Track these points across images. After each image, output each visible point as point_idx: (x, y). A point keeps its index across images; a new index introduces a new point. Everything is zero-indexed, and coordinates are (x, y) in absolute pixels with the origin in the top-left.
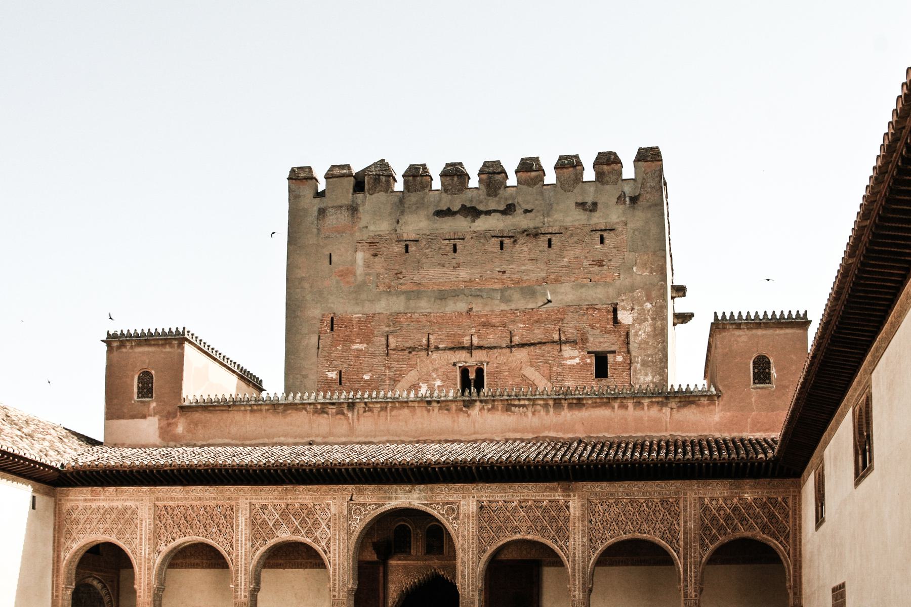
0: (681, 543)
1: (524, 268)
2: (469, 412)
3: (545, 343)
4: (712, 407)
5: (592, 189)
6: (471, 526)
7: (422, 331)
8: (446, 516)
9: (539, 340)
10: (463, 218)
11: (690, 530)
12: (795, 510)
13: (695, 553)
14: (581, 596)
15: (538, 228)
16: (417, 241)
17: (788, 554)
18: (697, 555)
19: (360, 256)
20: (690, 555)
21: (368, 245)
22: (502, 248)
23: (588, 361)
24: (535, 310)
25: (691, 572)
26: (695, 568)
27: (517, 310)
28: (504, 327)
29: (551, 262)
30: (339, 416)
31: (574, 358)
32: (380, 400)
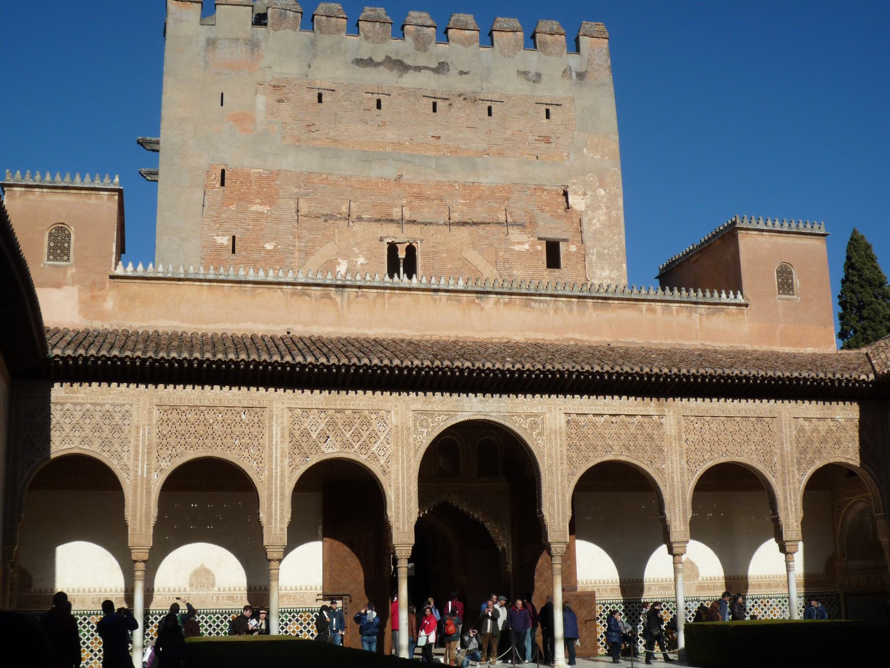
0: (778, 467)
1: (461, 135)
2: (482, 305)
3: (489, 223)
7: (341, 197)
8: (529, 431)
9: (483, 220)
11: (787, 453)
13: (793, 479)
14: (682, 529)
15: (477, 93)
16: (334, 90)
20: (789, 481)
22: (435, 110)
23: (539, 248)
24: (476, 184)
25: (790, 499)
29: (493, 132)
30: (324, 301)
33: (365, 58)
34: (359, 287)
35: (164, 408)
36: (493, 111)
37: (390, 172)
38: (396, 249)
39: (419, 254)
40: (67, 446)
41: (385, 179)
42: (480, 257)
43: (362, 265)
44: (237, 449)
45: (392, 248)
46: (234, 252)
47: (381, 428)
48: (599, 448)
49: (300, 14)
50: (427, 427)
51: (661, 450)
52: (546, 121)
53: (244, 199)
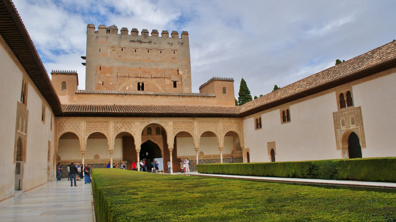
3: (160, 78)
4: (214, 99)
6: (171, 128)
10: (137, 43)
21: (111, 47)
22: (148, 52)
23: (172, 83)
26: (222, 138)
30: (122, 97)
31: (168, 82)
34: (130, 94)
35: (88, 122)
37: (138, 66)
38: (140, 84)
39: (144, 85)
40: (67, 130)
43: (132, 87)
44: (103, 130)
45: (139, 84)
46: (103, 85)
48: (180, 129)
50: (143, 125)
51: (193, 129)
52: (174, 54)
53: (105, 73)
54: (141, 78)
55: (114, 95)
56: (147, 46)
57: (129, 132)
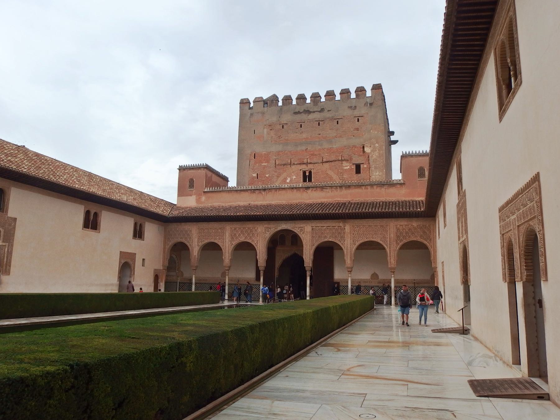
0: (388, 242)
1: (328, 132)
3: (336, 161)
5: (354, 101)
12: (433, 230)
17: (431, 247)
18: (395, 247)
19: (265, 130)
20: (392, 247)
21: (268, 126)
22: (319, 125)
23: (353, 167)
25: (392, 253)
26: (394, 252)
27: (325, 148)
28: (320, 155)
30: (260, 194)
31: (347, 166)
32: (274, 188)
33: (297, 111)
36: (339, 122)
37: (304, 148)
41: (302, 150)
42: (333, 172)
43: (294, 178)
45: (304, 173)
46: (257, 178)
47: (256, 233)
49: (277, 101)
52: (357, 123)
53: (261, 162)
54: (307, 164)
55: (249, 192)
56: (317, 116)
57: (249, 242)
